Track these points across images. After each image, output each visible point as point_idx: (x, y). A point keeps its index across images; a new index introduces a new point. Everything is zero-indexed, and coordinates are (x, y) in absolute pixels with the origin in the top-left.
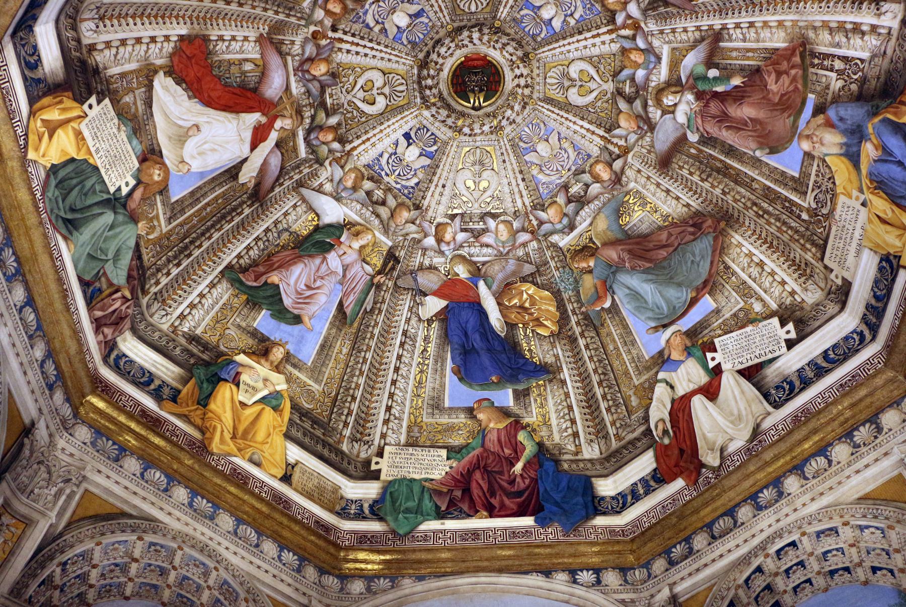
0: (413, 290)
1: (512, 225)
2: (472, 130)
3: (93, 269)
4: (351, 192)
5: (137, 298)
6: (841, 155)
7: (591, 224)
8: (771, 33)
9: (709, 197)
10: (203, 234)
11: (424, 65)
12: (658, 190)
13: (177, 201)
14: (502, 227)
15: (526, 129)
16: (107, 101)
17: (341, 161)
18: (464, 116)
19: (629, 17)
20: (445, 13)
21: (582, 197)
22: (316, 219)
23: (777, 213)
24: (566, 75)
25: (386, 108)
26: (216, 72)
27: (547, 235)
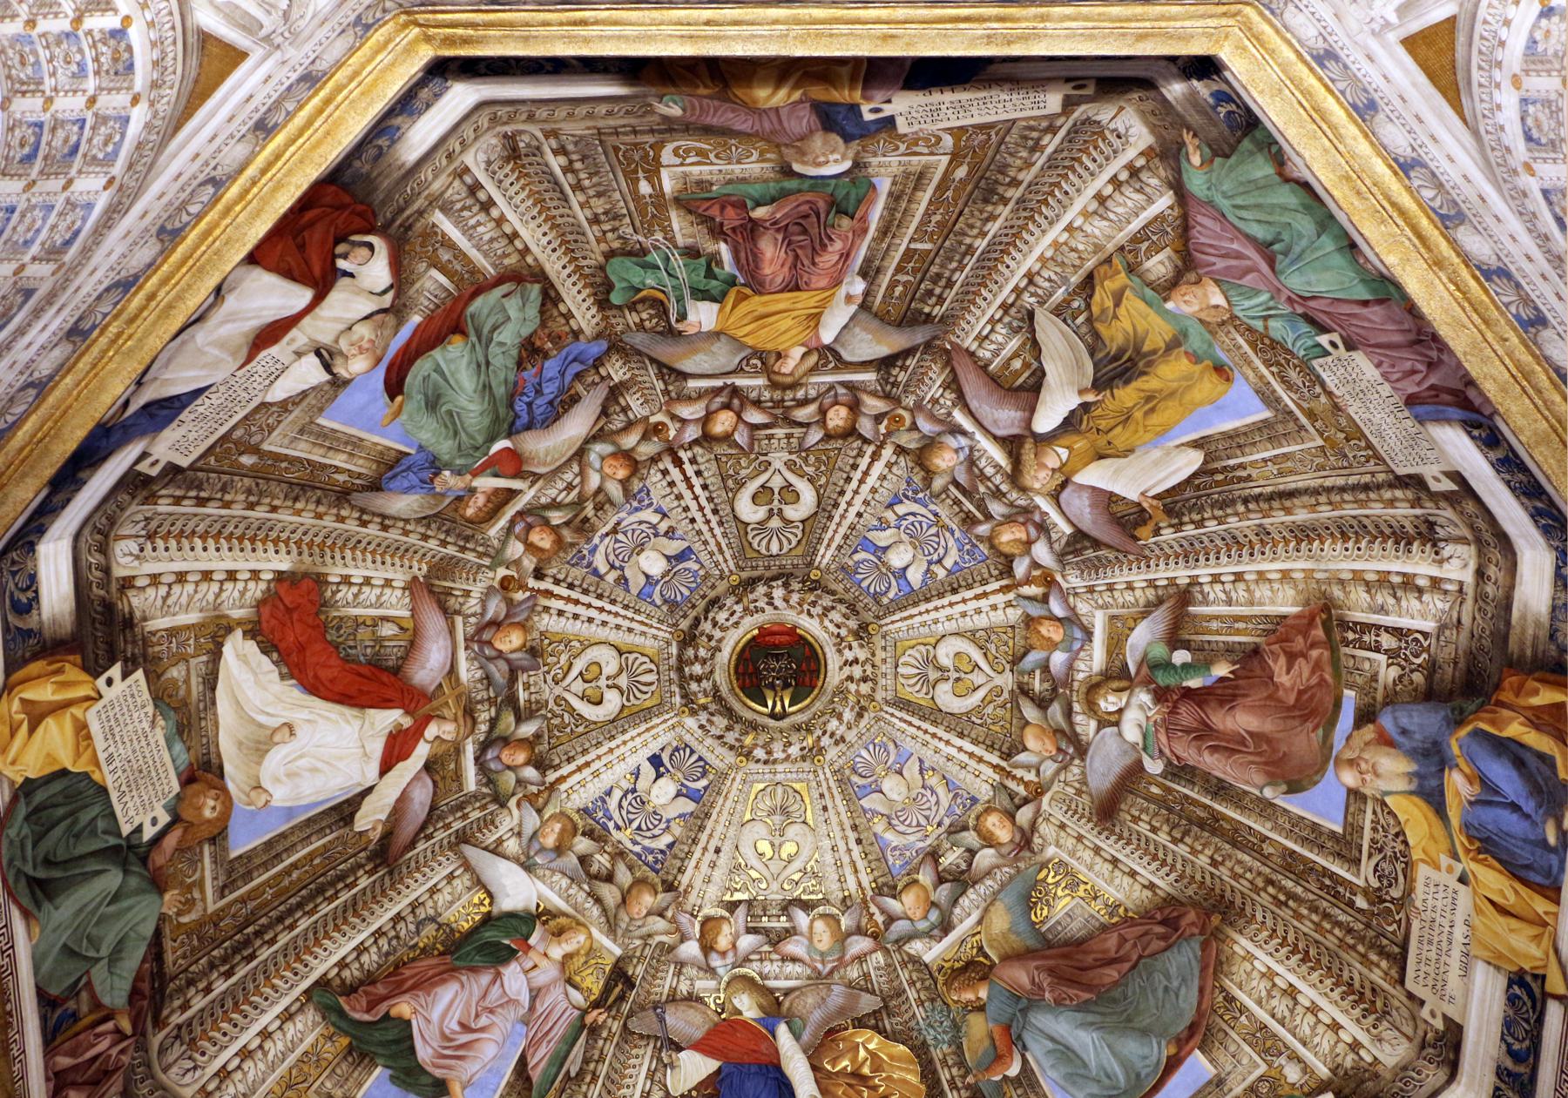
0: (657, 1038)
1: (838, 922)
2: (769, 753)
3: (69, 974)
4: (553, 855)
5: (144, 1034)
6: (1411, 793)
7: (980, 922)
8: (1272, 589)
9: (1188, 870)
10: (280, 919)
11: (688, 639)
12: (1098, 859)
13: (240, 857)
14: (820, 925)
15: (864, 753)
16: (139, 674)
17: (537, 801)
18: (755, 728)
19: (1035, 565)
20: (728, 557)
21: (963, 872)
22: (487, 902)
23: (1312, 897)
24: (931, 661)
25: (621, 711)
26: (331, 636)
27: (902, 941)
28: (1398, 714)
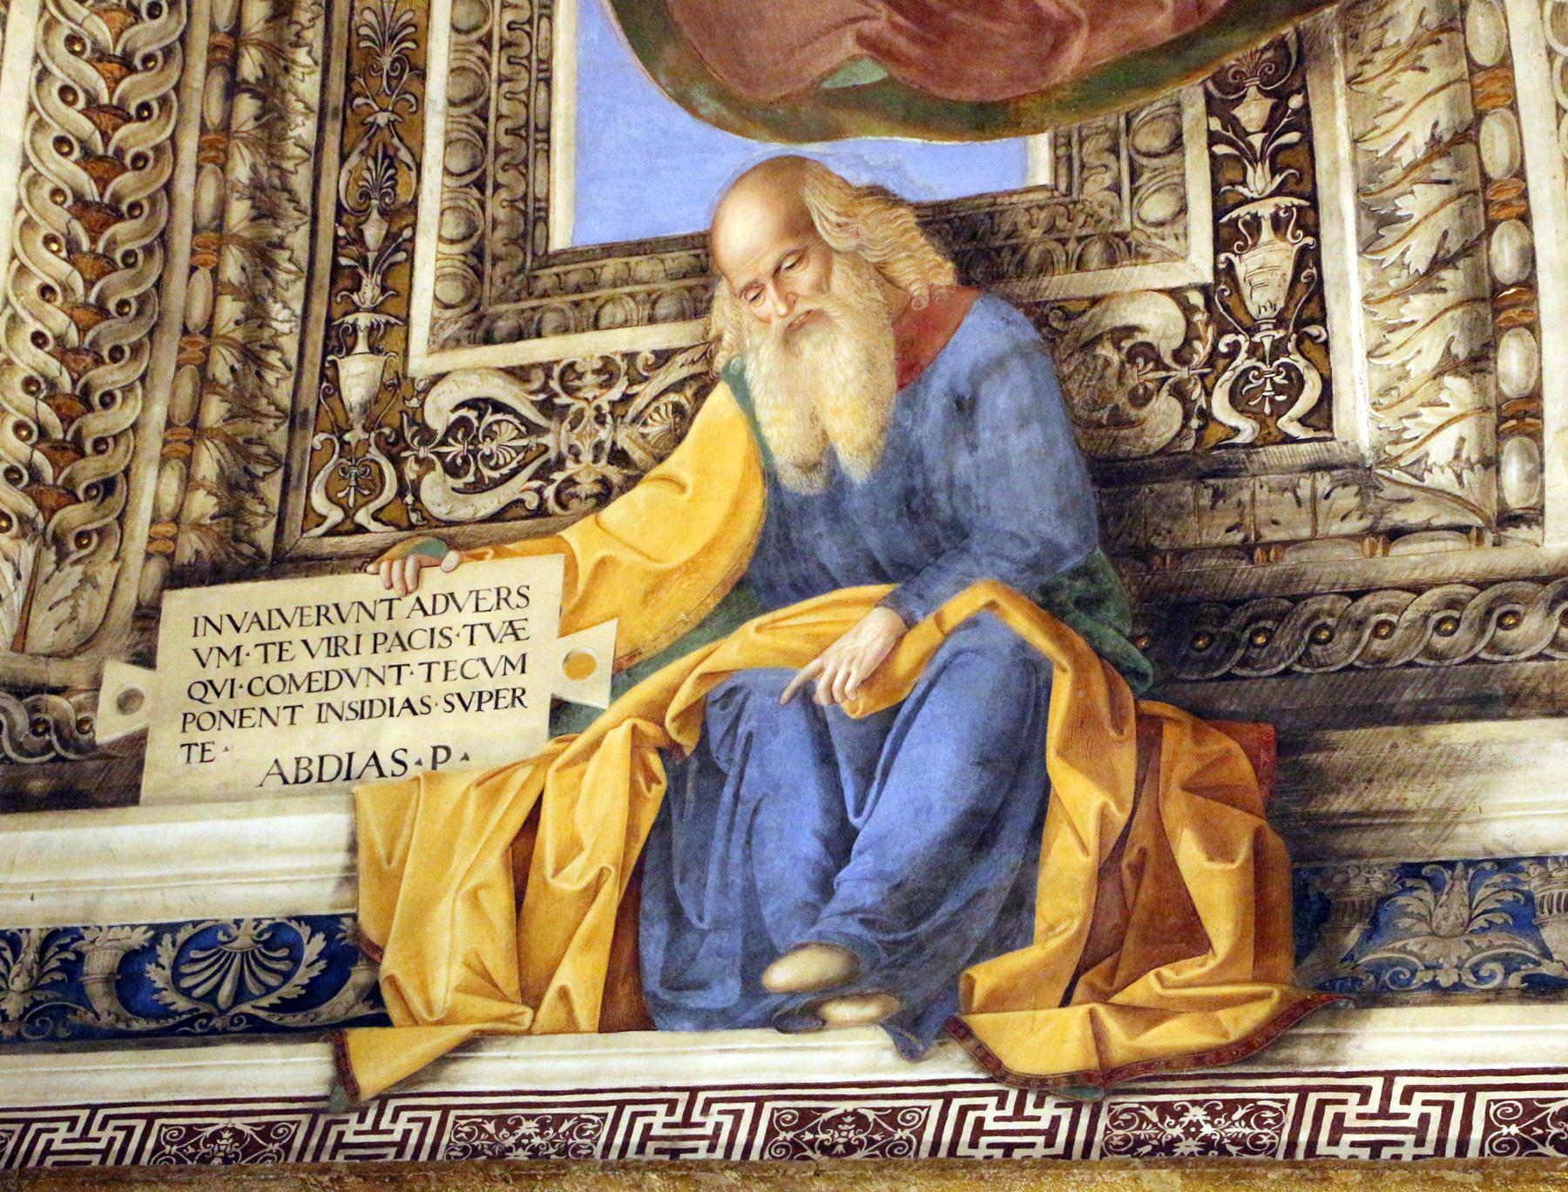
6: (771, 478)
23: (301, 181)
28: (1018, 373)
